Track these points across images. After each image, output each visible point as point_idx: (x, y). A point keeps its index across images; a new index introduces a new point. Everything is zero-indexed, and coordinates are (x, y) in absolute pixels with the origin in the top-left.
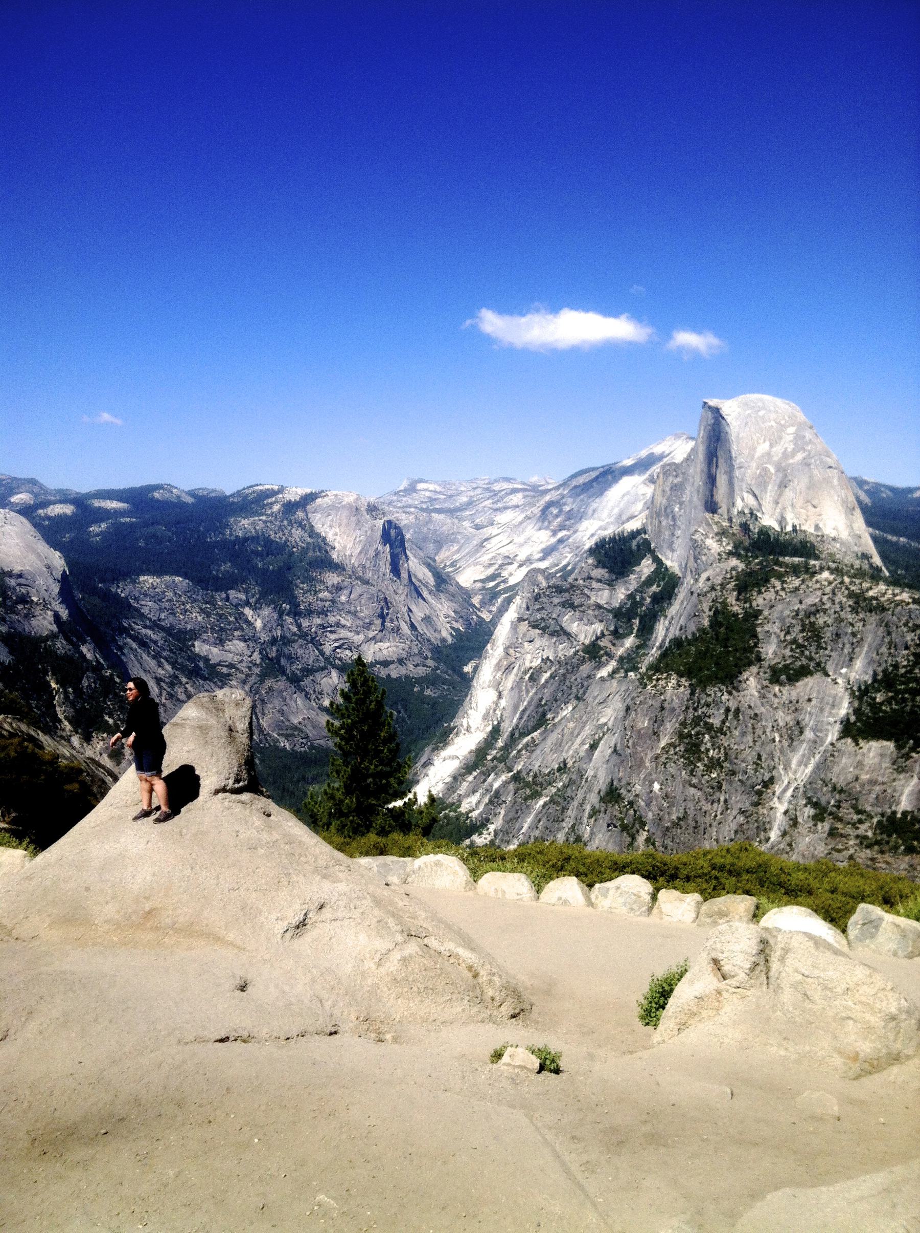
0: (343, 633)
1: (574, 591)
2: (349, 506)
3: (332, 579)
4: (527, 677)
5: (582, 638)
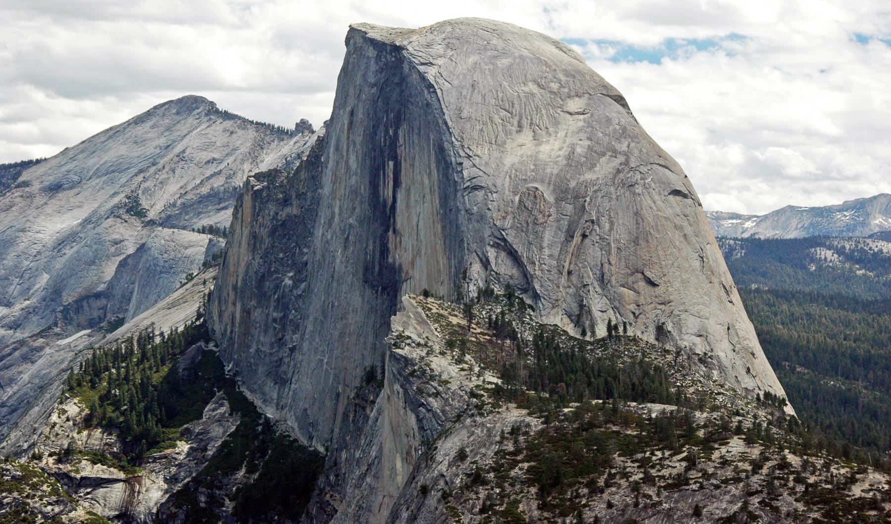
1: (34, 487)
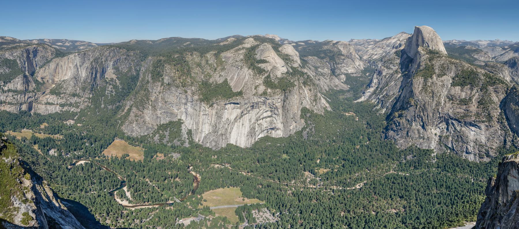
0: (345, 68)
2: (345, 44)
3: (343, 57)
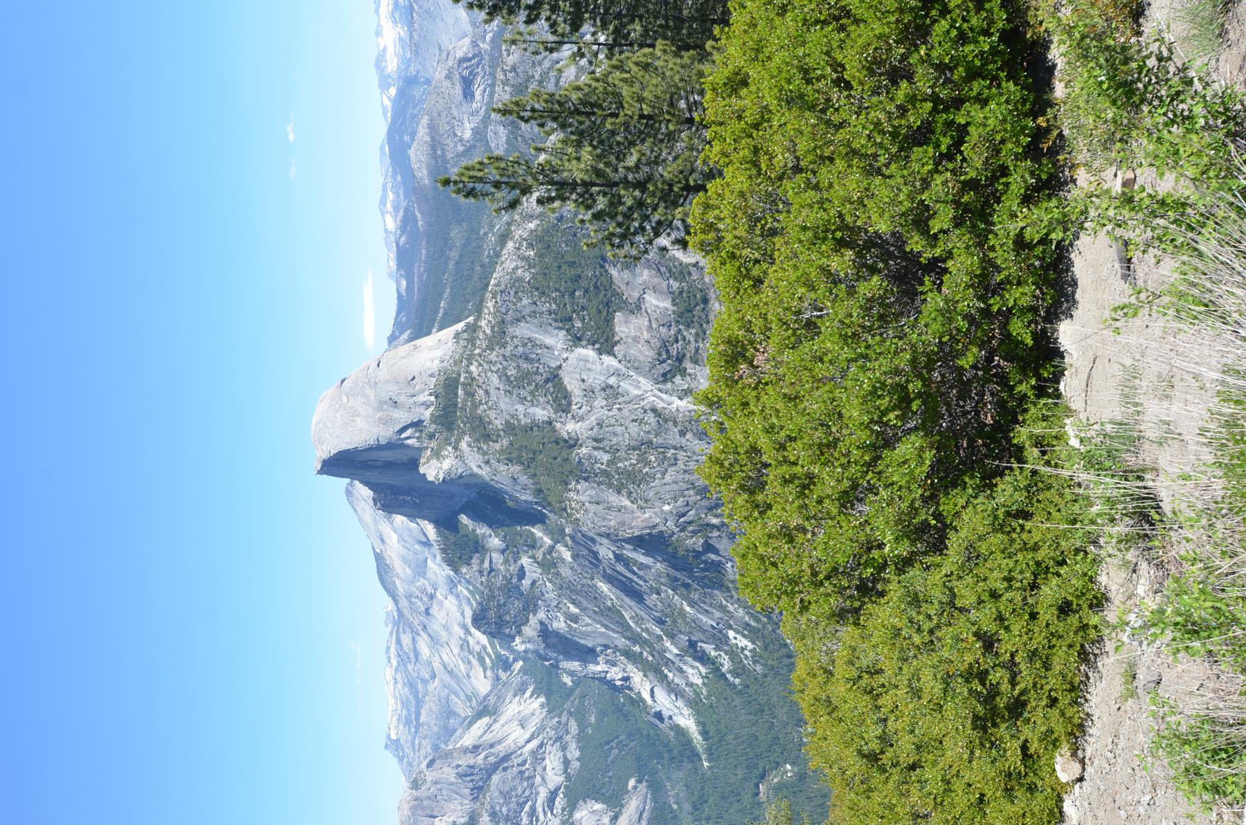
2: (414, 809)
4: (575, 626)
5: (535, 576)
